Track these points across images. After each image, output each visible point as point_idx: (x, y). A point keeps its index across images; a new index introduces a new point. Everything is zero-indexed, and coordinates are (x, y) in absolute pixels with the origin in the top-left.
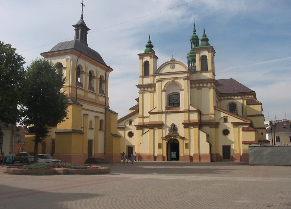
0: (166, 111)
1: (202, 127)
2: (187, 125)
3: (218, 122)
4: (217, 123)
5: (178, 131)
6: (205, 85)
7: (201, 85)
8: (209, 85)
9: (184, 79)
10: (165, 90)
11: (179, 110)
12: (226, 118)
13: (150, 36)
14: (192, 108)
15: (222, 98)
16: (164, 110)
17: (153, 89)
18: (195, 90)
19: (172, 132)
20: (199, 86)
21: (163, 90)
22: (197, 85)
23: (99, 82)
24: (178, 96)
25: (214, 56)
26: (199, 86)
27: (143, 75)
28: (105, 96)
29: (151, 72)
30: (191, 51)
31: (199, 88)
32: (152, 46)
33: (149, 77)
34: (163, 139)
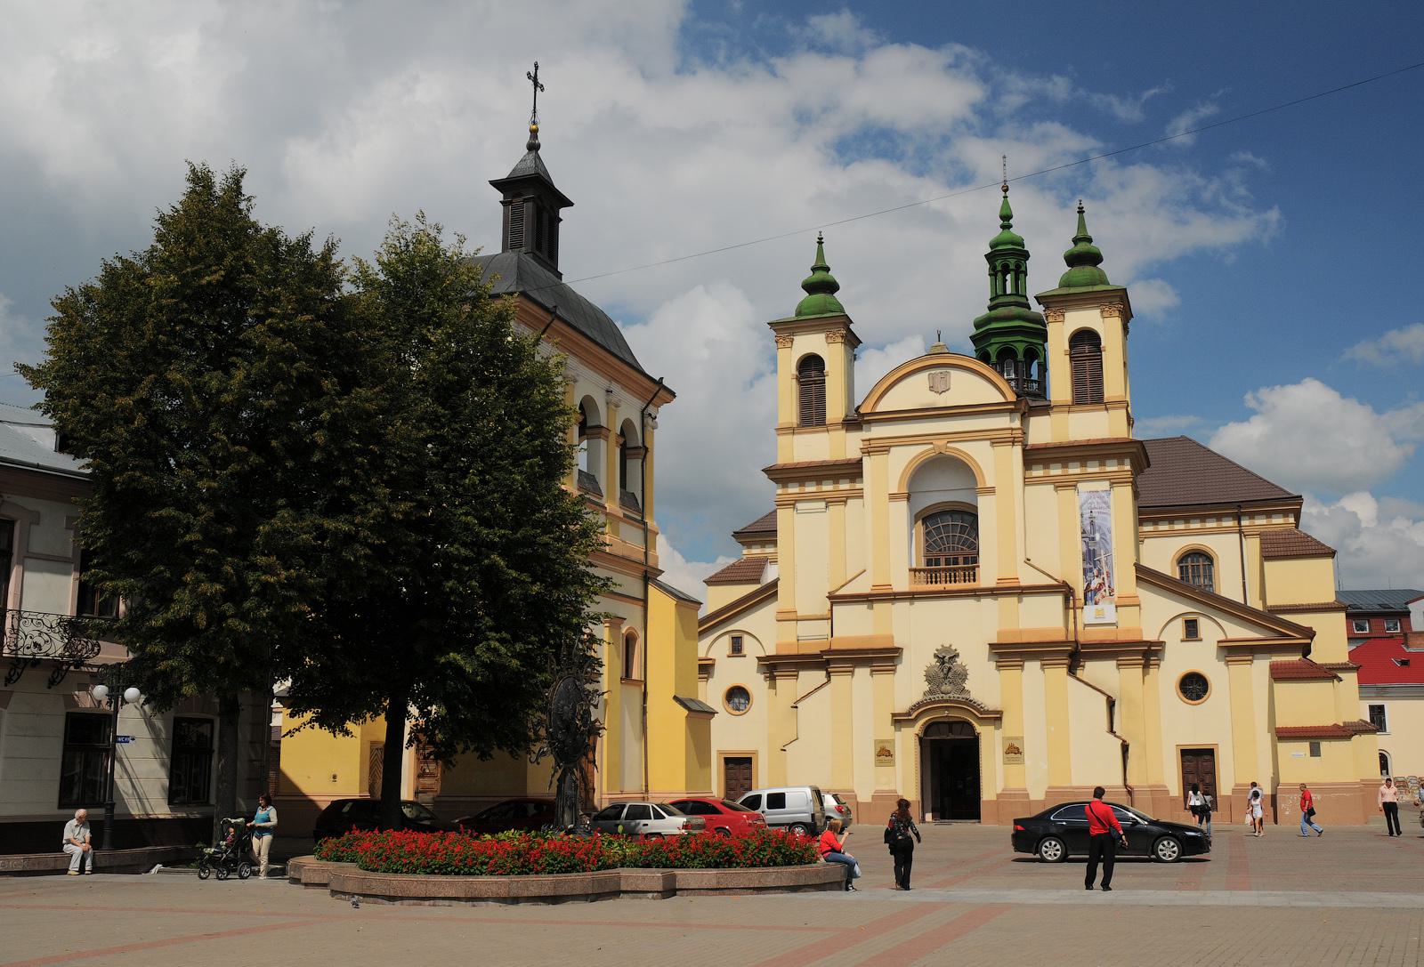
2: (1009, 653)
4: (1150, 644)
5: (967, 685)
6: (1093, 468)
7: (1074, 470)
8: (1112, 467)
9: (995, 442)
12: (1195, 621)
13: (821, 239)
14: (1029, 578)
15: (1148, 528)
17: (845, 486)
22: (1056, 471)
23: (618, 451)
24: (968, 516)
28: (645, 524)
29: (835, 408)
30: (990, 308)
32: (831, 287)
34: (899, 721)
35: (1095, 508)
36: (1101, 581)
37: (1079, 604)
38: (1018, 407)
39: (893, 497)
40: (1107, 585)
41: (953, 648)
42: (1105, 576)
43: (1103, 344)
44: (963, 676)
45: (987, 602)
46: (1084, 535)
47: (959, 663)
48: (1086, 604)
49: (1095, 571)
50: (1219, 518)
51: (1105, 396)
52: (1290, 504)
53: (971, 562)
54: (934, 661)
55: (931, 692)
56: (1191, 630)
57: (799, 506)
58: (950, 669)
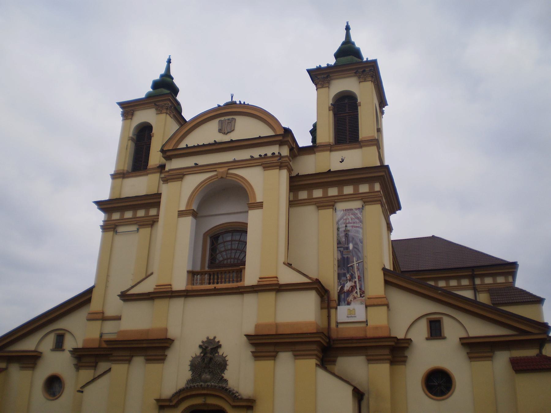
0: (190, 287)
1: (337, 357)
3: (401, 335)
5: (227, 375)
6: (348, 190)
7: (333, 192)
8: (364, 188)
10: (194, 207)
11: (239, 284)
14: (287, 276)
16: (180, 283)
17: (153, 212)
18: (309, 211)
19: (203, 376)
20: (325, 196)
21: (183, 208)
22: (318, 193)
25: (382, 113)
26: (325, 196)
27: (127, 166)
29: (155, 158)
31: (327, 204)
32: (175, 91)
33: (147, 174)
35: (349, 223)
36: (353, 284)
37: (333, 304)
38: (286, 139)
39: (182, 214)
40: (358, 288)
41: (217, 340)
42: (357, 280)
43: (359, 101)
44: (223, 365)
45: (250, 300)
46: (340, 246)
47: (221, 354)
48: (339, 305)
49: (348, 276)
50: (458, 278)
51: (360, 137)
52: (509, 268)
53: (238, 266)
54: (198, 352)
55: (192, 381)
56: (435, 330)
57: (120, 229)
58: (211, 359)
